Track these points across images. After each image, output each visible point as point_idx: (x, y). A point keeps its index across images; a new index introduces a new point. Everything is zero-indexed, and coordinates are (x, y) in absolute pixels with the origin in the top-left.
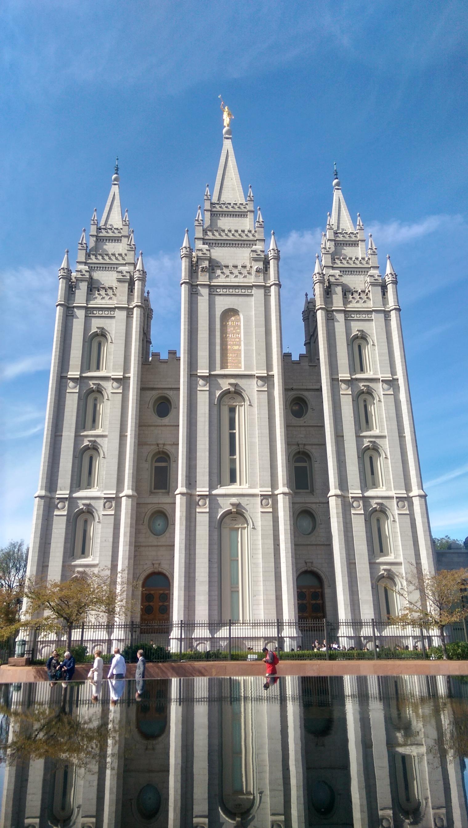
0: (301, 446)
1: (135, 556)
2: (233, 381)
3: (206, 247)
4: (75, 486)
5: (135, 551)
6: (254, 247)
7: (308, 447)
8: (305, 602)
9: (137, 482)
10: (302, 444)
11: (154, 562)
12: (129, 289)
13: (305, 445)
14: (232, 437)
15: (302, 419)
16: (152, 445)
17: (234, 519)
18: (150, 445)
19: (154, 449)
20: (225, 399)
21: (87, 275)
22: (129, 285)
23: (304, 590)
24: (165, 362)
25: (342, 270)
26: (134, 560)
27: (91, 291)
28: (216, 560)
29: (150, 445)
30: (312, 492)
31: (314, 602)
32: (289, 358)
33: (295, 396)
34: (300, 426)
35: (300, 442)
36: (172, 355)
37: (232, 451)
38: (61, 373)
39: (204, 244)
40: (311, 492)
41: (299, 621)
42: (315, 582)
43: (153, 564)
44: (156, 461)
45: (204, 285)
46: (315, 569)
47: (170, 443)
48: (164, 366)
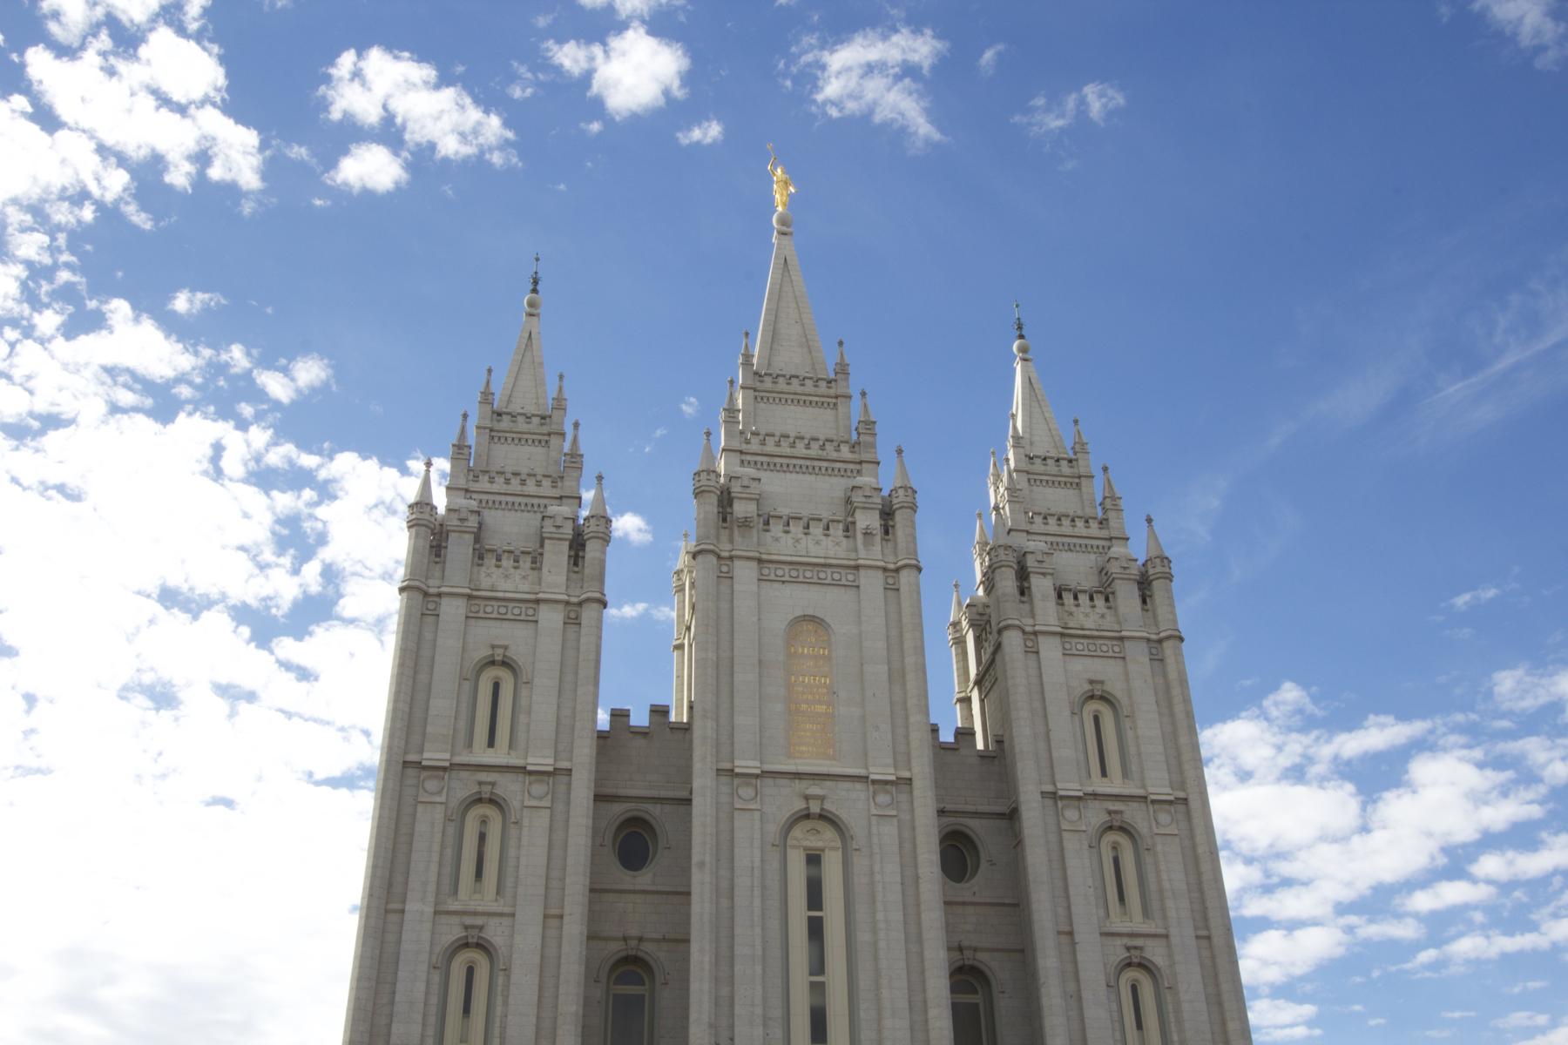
0: (968, 953)
2: (815, 790)
3: (751, 471)
6: (860, 480)
7: (982, 956)
10: (969, 948)
13: (975, 950)
14: (816, 929)
16: (615, 939)
18: (606, 939)
19: (614, 949)
20: (797, 832)
21: (473, 522)
22: (571, 547)
24: (642, 733)
27: (481, 557)
29: (606, 939)
34: (964, 904)
35: (965, 943)
38: (406, 752)
44: (619, 981)
45: (748, 558)
47: (655, 936)
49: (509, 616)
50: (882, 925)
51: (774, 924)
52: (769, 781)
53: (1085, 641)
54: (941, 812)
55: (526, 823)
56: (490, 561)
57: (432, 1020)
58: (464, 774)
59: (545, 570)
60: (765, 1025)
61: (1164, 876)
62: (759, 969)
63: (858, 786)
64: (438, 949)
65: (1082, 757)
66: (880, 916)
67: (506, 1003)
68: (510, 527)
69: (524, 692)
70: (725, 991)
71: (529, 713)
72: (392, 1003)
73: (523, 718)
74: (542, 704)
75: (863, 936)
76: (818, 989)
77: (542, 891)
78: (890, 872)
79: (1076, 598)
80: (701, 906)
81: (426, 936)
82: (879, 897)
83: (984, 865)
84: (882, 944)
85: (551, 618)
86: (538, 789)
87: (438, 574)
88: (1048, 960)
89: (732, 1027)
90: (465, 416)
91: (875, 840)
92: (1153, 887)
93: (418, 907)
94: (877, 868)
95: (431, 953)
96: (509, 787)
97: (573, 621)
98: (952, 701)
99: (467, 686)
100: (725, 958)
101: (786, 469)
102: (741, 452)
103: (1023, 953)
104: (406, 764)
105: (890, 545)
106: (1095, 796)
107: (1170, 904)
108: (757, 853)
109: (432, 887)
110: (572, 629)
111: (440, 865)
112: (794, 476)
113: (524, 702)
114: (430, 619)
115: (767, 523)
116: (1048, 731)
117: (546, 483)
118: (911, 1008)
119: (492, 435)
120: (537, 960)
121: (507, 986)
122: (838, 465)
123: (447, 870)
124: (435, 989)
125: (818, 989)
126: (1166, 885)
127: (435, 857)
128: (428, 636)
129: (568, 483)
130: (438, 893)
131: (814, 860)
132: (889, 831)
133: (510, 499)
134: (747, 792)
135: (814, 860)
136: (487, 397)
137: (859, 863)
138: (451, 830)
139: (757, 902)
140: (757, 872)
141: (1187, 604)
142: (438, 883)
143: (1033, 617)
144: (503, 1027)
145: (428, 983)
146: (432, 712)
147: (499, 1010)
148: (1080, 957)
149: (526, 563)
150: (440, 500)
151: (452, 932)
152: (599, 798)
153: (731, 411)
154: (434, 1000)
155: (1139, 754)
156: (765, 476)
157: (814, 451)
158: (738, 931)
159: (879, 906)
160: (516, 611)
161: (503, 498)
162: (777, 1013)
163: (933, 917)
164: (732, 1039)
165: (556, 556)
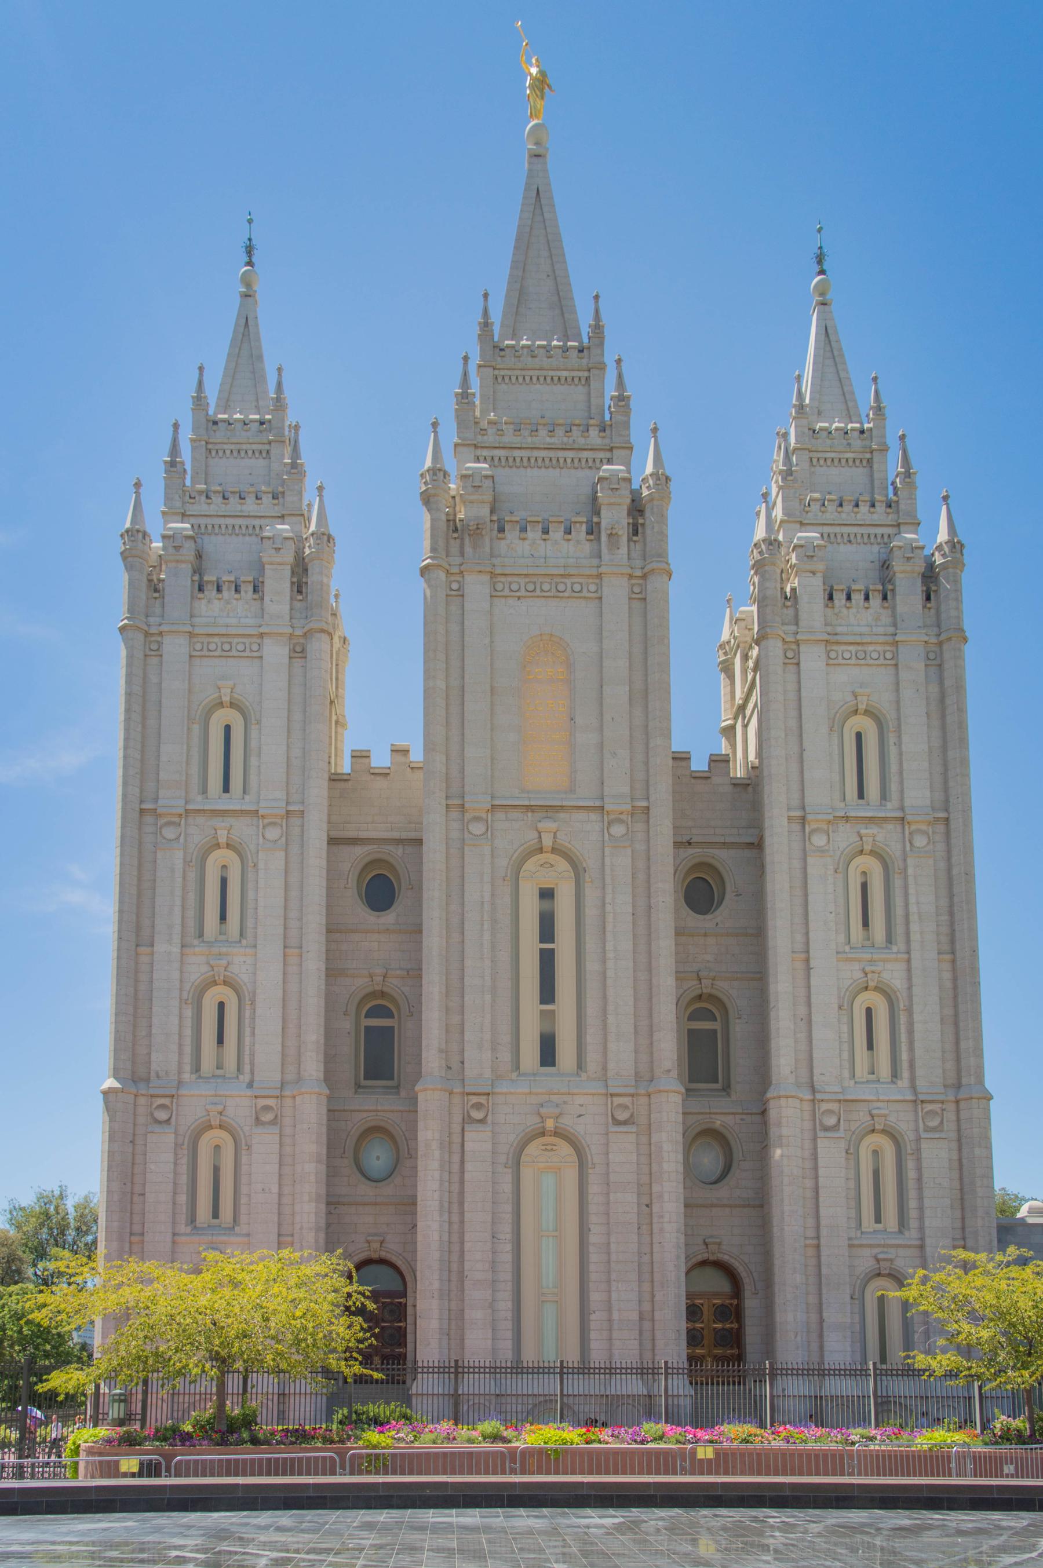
1: (328, 1225)
4: (187, 1068)
5: (329, 1213)
8: (699, 1325)
9: (326, 1063)
11: (370, 1238)
12: (292, 583)
14: (547, 961)
15: (708, 917)
17: (549, 1147)
20: (530, 865)
23: (698, 1302)
25: (827, 530)
26: (327, 1233)
27: (201, 589)
28: (509, 1236)
30: (727, 1088)
31: (719, 1326)
32: (684, 763)
33: (697, 860)
36: (400, 758)
37: (547, 992)
38: (141, 802)
39: (477, 460)
40: (724, 1089)
41: (691, 1365)
42: (723, 1285)
43: (368, 1242)
46: (726, 1258)
48: (380, 783)
49: (234, 653)
50: (610, 955)
51: (504, 956)
52: (500, 815)
53: (851, 648)
54: (677, 845)
55: (261, 865)
56: (211, 592)
57: (188, 1049)
58: (200, 820)
59: (267, 598)
60: (494, 1050)
61: (912, 899)
62: (488, 998)
63: (594, 816)
64: (187, 986)
65: (836, 777)
66: (609, 946)
67: (253, 1034)
68: (228, 553)
69: (254, 733)
70: (456, 1019)
71: (259, 755)
72: (149, 1035)
73: (253, 761)
74: (271, 748)
75: (592, 966)
76: (548, 1017)
77: (281, 930)
78: (621, 904)
79: (849, 598)
80: (433, 941)
81: (176, 975)
82: (609, 927)
83: (729, 895)
84: (610, 973)
85: (276, 652)
86: (273, 833)
87: (158, 610)
88: (782, 985)
89: (462, 1052)
90: (176, 426)
91: (608, 871)
92: (899, 911)
93: (167, 948)
94: (608, 900)
95: (181, 990)
96: (243, 830)
97: (299, 652)
98: (710, 714)
99: (196, 728)
100: (456, 988)
101: (528, 463)
102: (476, 446)
103: (759, 977)
104: (142, 811)
105: (638, 546)
106: (847, 819)
107: (914, 927)
108: (487, 888)
109: (177, 929)
110: (298, 663)
111: (183, 907)
112: (536, 471)
113: (253, 744)
114: (154, 660)
115: (501, 530)
116: (802, 750)
117: (267, 499)
118: (636, 1032)
119: (207, 448)
120: (280, 993)
121: (253, 1019)
122: (585, 454)
123: (191, 913)
124: (188, 1022)
125: (548, 1017)
126: (913, 908)
127: (178, 902)
128: (154, 679)
129: (290, 498)
130: (183, 935)
131: (547, 894)
132: (621, 863)
133: (230, 521)
134: (477, 828)
135: (547, 894)
136: (199, 401)
137: (591, 895)
138: (192, 875)
139: (487, 936)
140: (487, 907)
141: (976, 599)
142: (183, 925)
143: (797, 624)
144: (252, 1055)
145: (181, 1017)
146: (164, 758)
147: (247, 1040)
148: (813, 982)
149: (247, 590)
150: (158, 527)
151: (197, 969)
152: (332, 841)
153: (465, 397)
154: (188, 1032)
155: (901, 772)
156: (501, 473)
157: (559, 438)
158: (468, 963)
159: (609, 936)
160: (241, 647)
161: (222, 521)
162: (506, 1038)
163: (665, 945)
164: (463, 1063)
165: (278, 584)
